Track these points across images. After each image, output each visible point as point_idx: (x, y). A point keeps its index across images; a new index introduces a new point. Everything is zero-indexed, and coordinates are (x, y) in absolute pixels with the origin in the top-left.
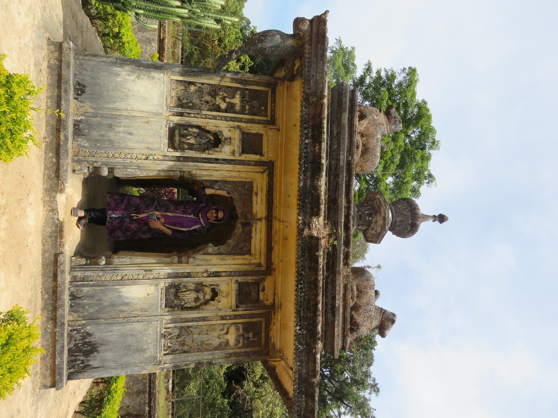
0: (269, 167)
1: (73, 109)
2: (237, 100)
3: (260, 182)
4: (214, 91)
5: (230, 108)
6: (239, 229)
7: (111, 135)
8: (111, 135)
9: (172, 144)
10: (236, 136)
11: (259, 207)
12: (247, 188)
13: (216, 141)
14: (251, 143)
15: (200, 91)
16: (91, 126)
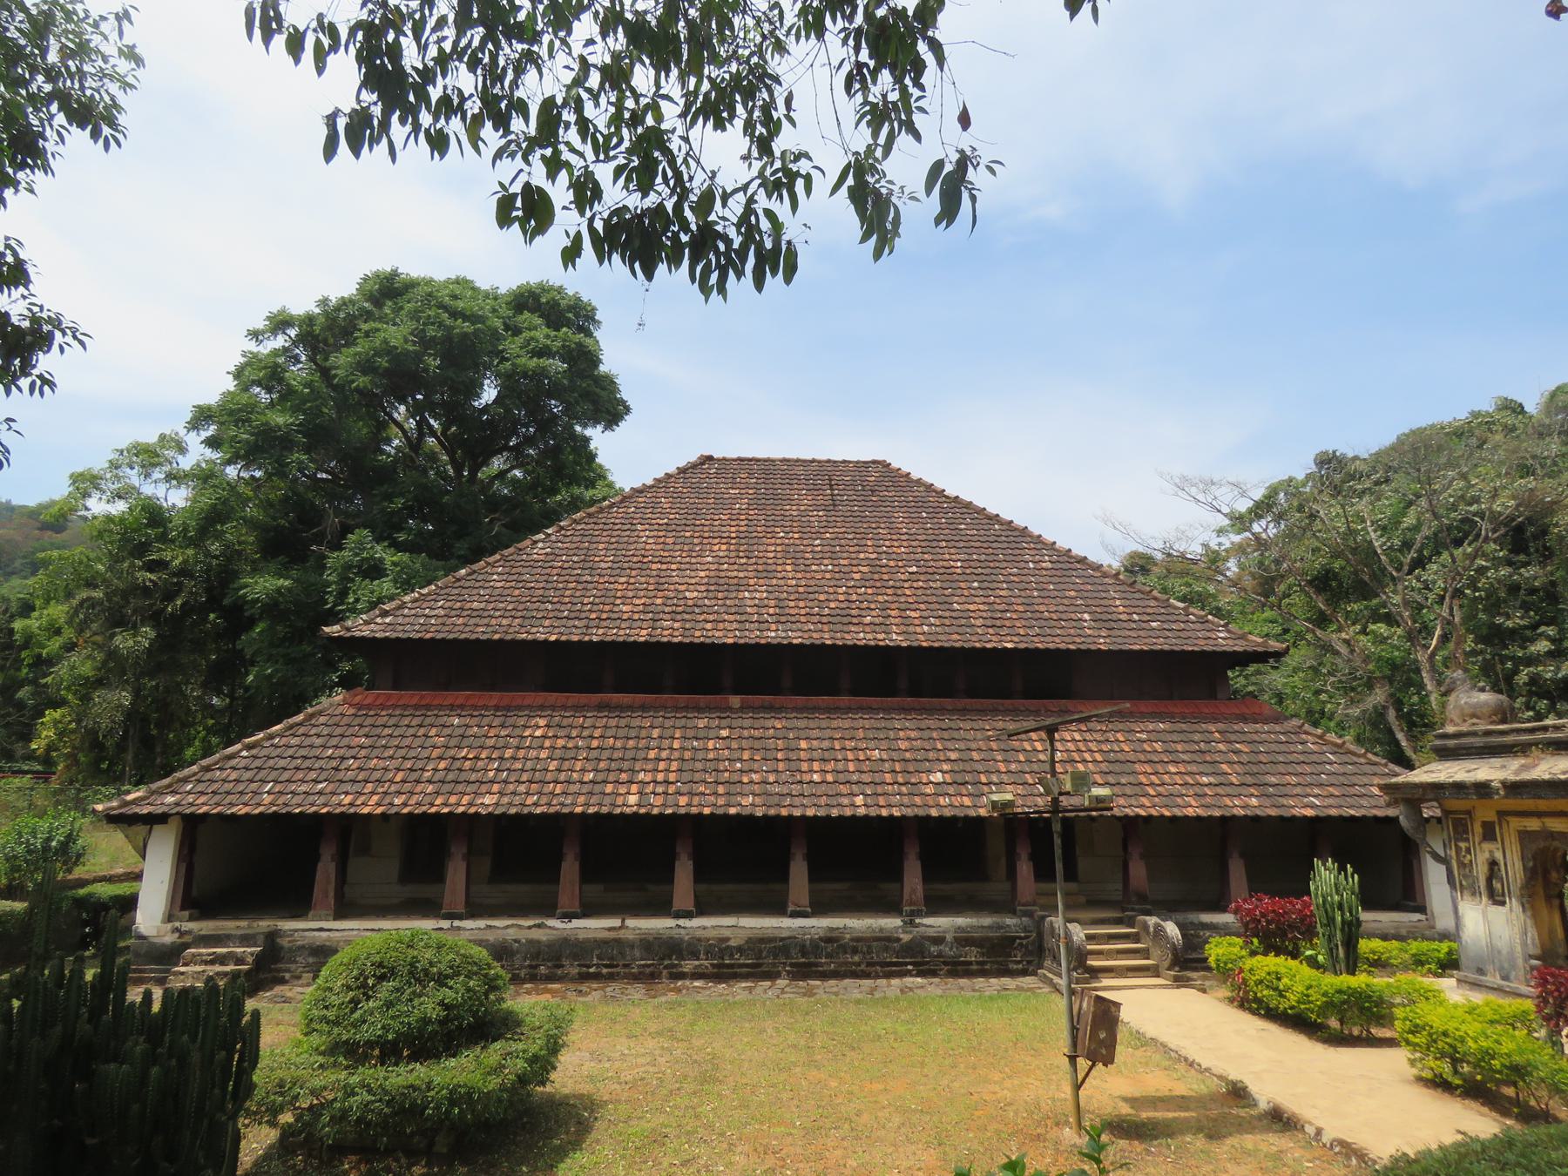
0: (1502, 814)
1: (1493, 979)
2: (1463, 845)
3: (1516, 823)
4: (1462, 865)
5: (1468, 851)
6: (1556, 844)
7: (1504, 952)
8: (1504, 952)
9: (1503, 903)
10: (1487, 846)
11: (1533, 824)
12: (1524, 836)
13: (1493, 864)
14: (1489, 834)
15: (1465, 876)
16: (1501, 969)
